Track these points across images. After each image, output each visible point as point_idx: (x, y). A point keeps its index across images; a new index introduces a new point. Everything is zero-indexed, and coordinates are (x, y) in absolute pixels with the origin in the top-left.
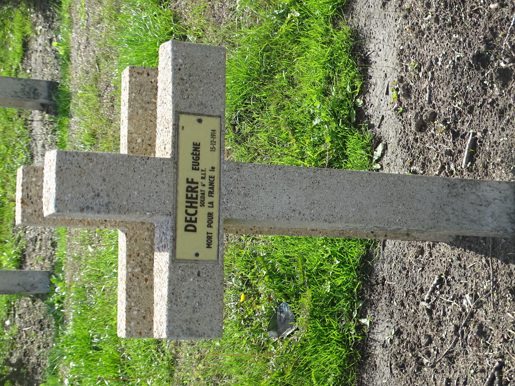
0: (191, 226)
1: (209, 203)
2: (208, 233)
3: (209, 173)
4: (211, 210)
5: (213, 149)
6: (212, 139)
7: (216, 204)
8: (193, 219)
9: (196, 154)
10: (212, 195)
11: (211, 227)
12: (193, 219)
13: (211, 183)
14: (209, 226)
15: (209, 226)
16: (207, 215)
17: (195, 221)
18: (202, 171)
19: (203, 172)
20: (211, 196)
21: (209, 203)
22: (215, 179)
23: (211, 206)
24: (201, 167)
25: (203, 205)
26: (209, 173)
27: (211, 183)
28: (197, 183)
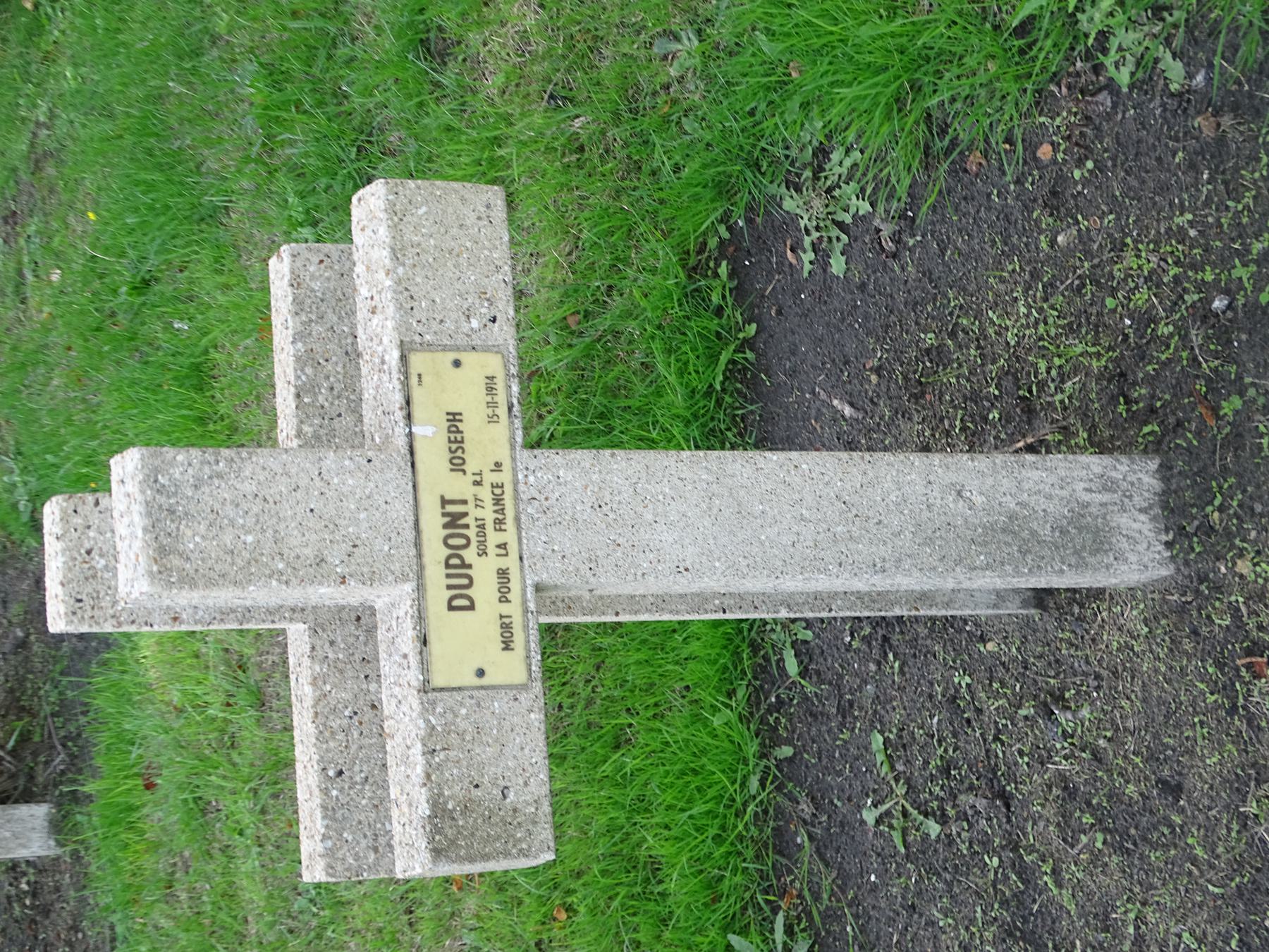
0: (461, 602)
1: (499, 546)
2: (501, 617)
3: (489, 477)
4: (503, 563)
6: (489, 399)
10: (503, 527)
11: (508, 601)
13: (498, 501)
14: (504, 599)
15: (504, 599)
16: (495, 575)
20: (501, 530)
21: (499, 546)
22: (508, 489)
23: (503, 552)
24: (471, 467)
26: (489, 477)
27: (498, 501)
28: (465, 502)
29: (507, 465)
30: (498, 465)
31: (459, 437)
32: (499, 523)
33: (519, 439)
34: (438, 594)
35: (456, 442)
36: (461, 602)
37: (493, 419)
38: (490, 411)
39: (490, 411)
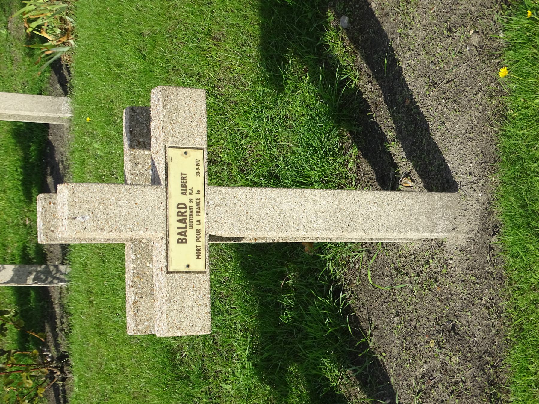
0: (182, 241)
1: (197, 221)
2: (197, 247)
4: (199, 227)
5: (198, 174)
6: (197, 167)
7: (202, 221)
9: (183, 182)
11: (199, 241)
13: (198, 205)
14: (198, 240)
15: (198, 240)
21: (197, 221)
25: (191, 222)
27: (198, 205)
30: (199, 192)
31: (185, 181)
34: (174, 237)
36: (182, 241)
38: (197, 171)
39: (197, 171)
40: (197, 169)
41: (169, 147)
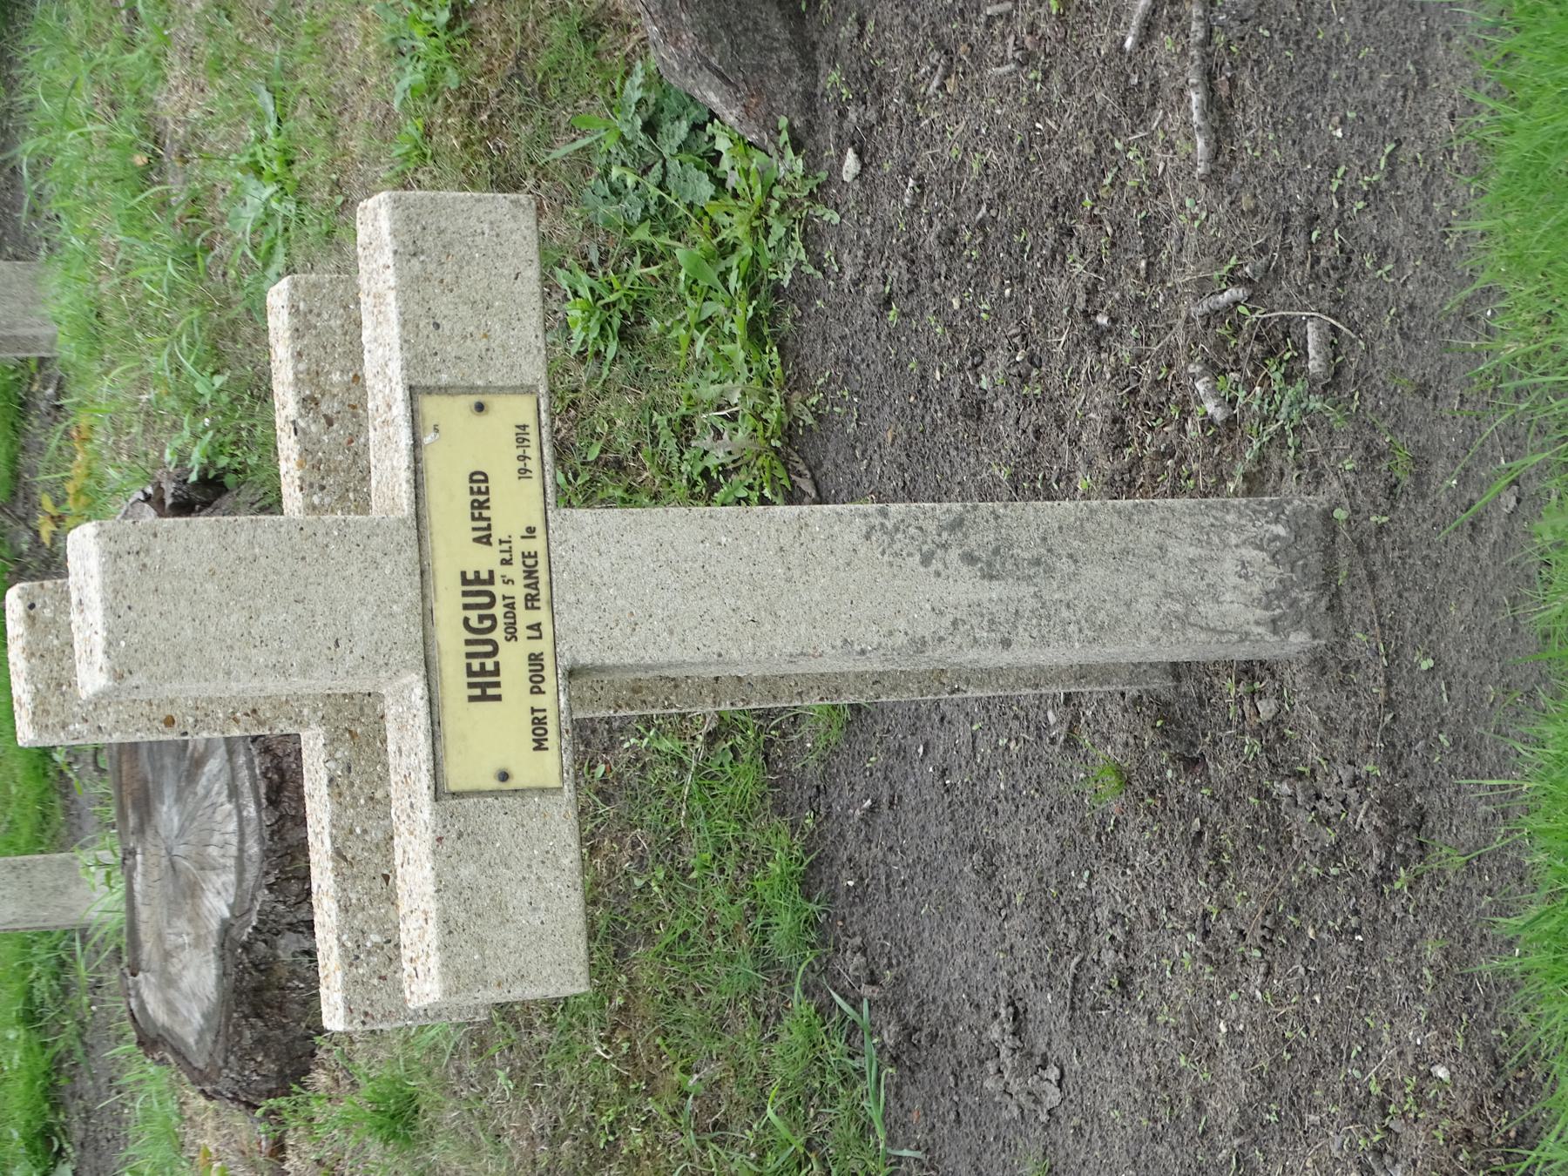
1: (530, 627)
2: (533, 711)
3: (520, 546)
6: (520, 451)
7: (547, 629)
8: (490, 666)
11: (541, 692)
12: (490, 666)
13: (530, 573)
14: (536, 690)
15: (536, 690)
16: (526, 662)
17: (496, 672)
18: (501, 542)
19: (505, 547)
20: (533, 608)
21: (530, 627)
22: (542, 560)
23: (536, 634)
24: (497, 533)
26: (520, 546)
29: (540, 532)
32: (531, 601)
33: (551, 499)
35: (479, 506)
37: (524, 473)
38: (521, 465)
39: (521, 465)
40: (523, 458)
41: (429, 391)
